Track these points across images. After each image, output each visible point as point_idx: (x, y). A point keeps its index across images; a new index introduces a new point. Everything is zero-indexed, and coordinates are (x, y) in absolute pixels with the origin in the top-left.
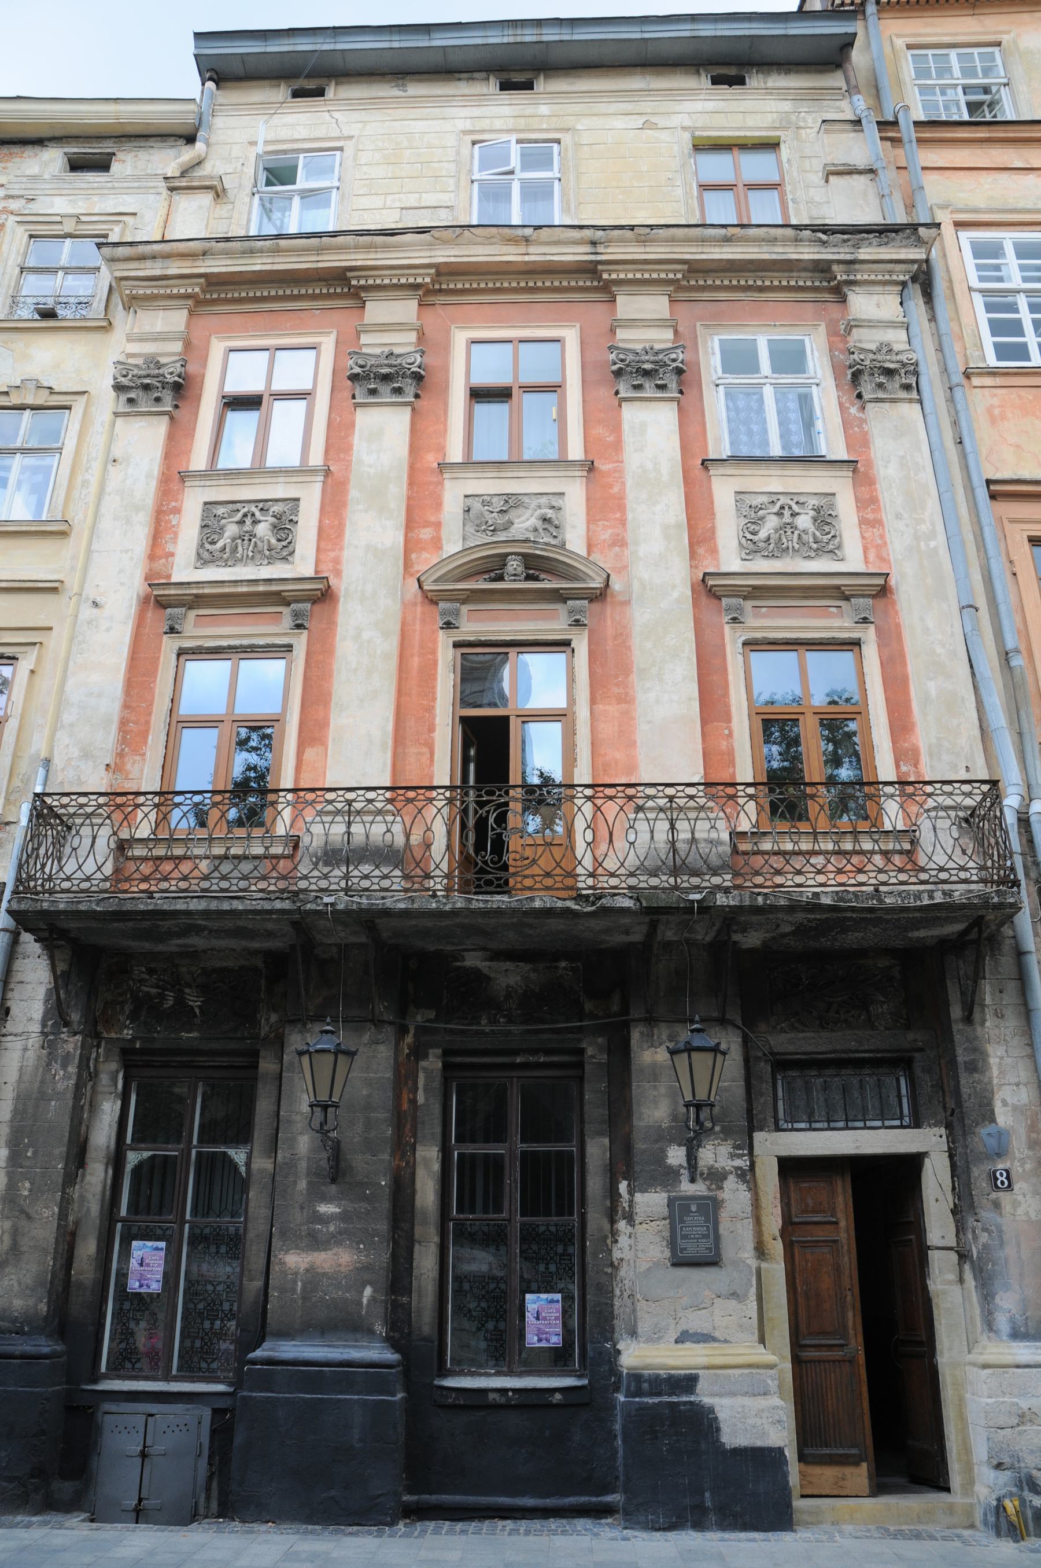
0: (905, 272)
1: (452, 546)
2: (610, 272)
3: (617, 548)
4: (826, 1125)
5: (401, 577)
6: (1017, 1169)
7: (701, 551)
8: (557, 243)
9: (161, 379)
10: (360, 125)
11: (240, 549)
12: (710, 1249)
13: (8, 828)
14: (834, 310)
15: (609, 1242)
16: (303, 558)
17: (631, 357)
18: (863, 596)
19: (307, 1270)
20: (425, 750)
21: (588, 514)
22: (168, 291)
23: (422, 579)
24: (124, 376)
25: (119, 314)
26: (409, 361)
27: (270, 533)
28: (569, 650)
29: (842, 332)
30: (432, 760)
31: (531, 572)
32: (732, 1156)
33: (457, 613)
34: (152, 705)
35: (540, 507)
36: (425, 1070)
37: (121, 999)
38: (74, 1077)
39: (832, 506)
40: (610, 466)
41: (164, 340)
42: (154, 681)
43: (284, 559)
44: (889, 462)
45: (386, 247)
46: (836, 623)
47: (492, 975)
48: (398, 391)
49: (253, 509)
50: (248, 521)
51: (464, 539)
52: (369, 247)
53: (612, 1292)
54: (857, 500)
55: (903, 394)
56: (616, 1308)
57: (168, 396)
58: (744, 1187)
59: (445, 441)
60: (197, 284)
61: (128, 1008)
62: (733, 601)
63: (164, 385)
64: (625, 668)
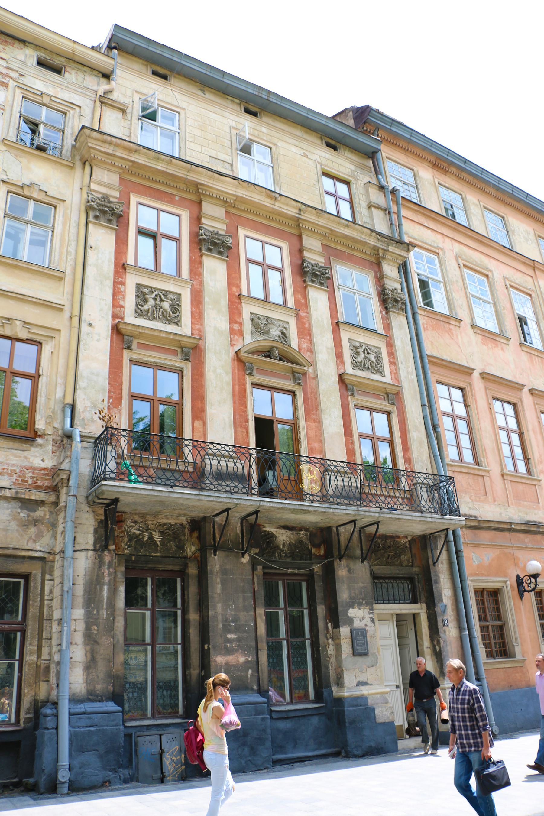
6: (449, 619)
8: (287, 205)
9: (111, 209)
10: (186, 104)
11: (155, 312)
13: (46, 437)
15: (327, 647)
16: (185, 325)
20: (244, 430)
32: (370, 613)
36: (257, 575)
37: (121, 535)
41: (110, 188)
42: (122, 372)
43: (177, 324)
45: (218, 180)
47: (277, 535)
48: (220, 253)
49: (160, 293)
52: (211, 178)
59: (240, 282)
61: (126, 539)
64: (317, 407)
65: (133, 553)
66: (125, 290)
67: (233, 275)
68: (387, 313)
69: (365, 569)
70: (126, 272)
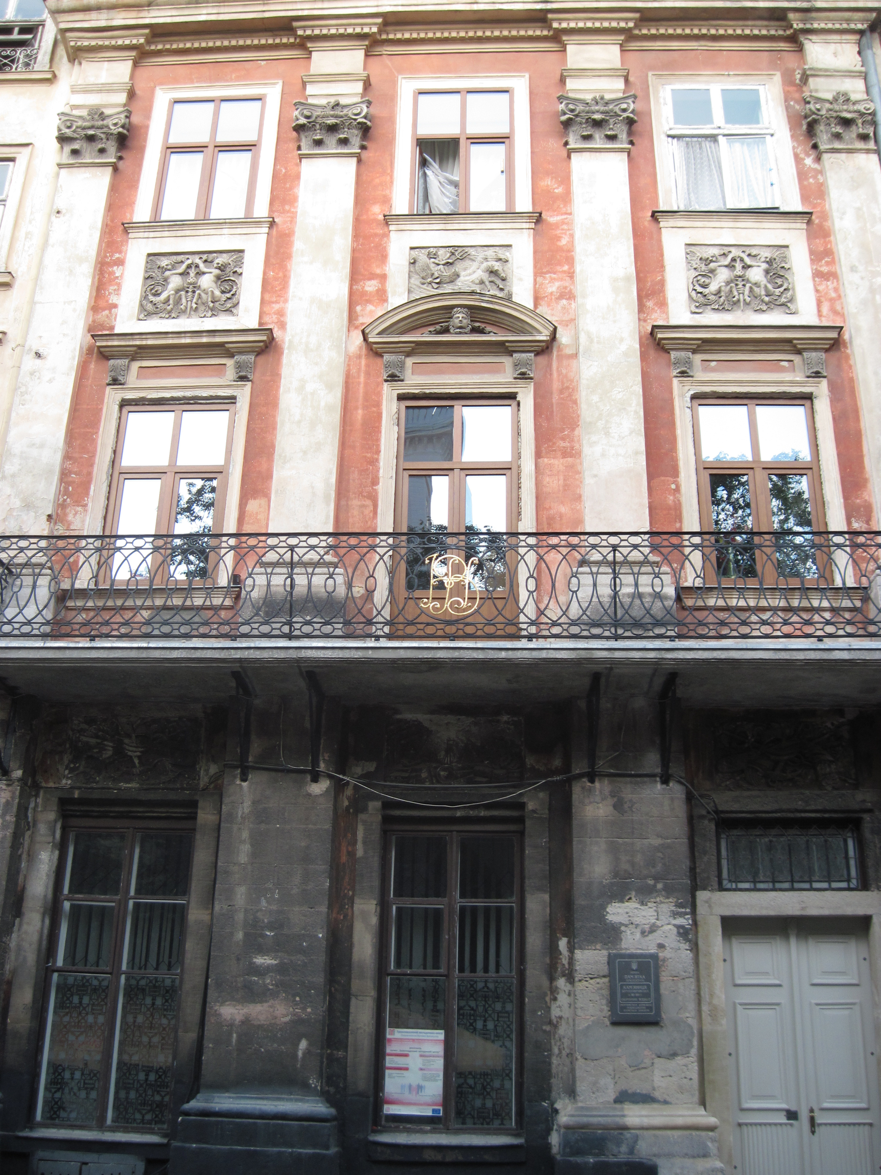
0: (862, 21)
1: (397, 297)
2: (560, 20)
3: (564, 302)
4: (770, 885)
5: (345, 329)
7: (650, 304)
9: (105, 130)
11: (184, 301)
12: (650, 1008)
14: (791, 60)
15: (548, 999)
17: (580, 108)
18: (815, 350)
19: (243, 1022)
20: (368, 502)
21: (535, 266)
22: (113, 42)
23: (367, 331)
24: (69, 127)
25: (63, 67)
26: (356, 112)
27: (214, 285)
28: (514, 403)
29: (798, 81)
30: (375, 512)
31: (477, 324)
32: (675, 915)
33: (402, 366)
34: (94, 456)
35: (486, 259)
38: (12, 826)
39: (784, 259)
40: (559, 218)
41: (108, 91)
42: (97, 433)
43: (229, 311)
44: (844, 213)
46: (787, 377)
48: (344, 142)
49: (197, 261)
50: (192, 272)
51: (409, 291)
53: (550, 1050)
54: (812, 252)
55: (860, 145)
56: (554, 1066)
57: (112, 147)
58: (687, 946)
60: (142, 35)
62: (683, 354)
63: (108, 136)
64: (572, 422)
65: (78, 785)
66: (122, 274)
67: (377, 181)
68: (818, 159)
69: (672, 799)
70: (127, 242)
